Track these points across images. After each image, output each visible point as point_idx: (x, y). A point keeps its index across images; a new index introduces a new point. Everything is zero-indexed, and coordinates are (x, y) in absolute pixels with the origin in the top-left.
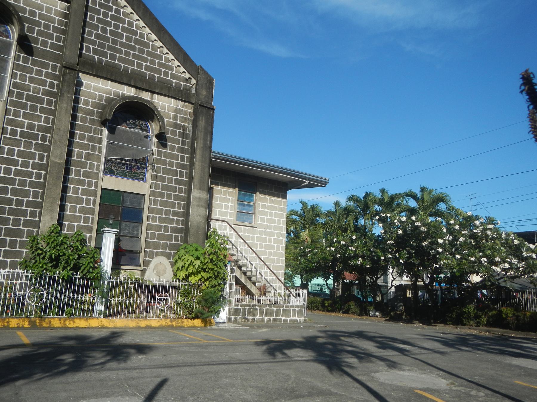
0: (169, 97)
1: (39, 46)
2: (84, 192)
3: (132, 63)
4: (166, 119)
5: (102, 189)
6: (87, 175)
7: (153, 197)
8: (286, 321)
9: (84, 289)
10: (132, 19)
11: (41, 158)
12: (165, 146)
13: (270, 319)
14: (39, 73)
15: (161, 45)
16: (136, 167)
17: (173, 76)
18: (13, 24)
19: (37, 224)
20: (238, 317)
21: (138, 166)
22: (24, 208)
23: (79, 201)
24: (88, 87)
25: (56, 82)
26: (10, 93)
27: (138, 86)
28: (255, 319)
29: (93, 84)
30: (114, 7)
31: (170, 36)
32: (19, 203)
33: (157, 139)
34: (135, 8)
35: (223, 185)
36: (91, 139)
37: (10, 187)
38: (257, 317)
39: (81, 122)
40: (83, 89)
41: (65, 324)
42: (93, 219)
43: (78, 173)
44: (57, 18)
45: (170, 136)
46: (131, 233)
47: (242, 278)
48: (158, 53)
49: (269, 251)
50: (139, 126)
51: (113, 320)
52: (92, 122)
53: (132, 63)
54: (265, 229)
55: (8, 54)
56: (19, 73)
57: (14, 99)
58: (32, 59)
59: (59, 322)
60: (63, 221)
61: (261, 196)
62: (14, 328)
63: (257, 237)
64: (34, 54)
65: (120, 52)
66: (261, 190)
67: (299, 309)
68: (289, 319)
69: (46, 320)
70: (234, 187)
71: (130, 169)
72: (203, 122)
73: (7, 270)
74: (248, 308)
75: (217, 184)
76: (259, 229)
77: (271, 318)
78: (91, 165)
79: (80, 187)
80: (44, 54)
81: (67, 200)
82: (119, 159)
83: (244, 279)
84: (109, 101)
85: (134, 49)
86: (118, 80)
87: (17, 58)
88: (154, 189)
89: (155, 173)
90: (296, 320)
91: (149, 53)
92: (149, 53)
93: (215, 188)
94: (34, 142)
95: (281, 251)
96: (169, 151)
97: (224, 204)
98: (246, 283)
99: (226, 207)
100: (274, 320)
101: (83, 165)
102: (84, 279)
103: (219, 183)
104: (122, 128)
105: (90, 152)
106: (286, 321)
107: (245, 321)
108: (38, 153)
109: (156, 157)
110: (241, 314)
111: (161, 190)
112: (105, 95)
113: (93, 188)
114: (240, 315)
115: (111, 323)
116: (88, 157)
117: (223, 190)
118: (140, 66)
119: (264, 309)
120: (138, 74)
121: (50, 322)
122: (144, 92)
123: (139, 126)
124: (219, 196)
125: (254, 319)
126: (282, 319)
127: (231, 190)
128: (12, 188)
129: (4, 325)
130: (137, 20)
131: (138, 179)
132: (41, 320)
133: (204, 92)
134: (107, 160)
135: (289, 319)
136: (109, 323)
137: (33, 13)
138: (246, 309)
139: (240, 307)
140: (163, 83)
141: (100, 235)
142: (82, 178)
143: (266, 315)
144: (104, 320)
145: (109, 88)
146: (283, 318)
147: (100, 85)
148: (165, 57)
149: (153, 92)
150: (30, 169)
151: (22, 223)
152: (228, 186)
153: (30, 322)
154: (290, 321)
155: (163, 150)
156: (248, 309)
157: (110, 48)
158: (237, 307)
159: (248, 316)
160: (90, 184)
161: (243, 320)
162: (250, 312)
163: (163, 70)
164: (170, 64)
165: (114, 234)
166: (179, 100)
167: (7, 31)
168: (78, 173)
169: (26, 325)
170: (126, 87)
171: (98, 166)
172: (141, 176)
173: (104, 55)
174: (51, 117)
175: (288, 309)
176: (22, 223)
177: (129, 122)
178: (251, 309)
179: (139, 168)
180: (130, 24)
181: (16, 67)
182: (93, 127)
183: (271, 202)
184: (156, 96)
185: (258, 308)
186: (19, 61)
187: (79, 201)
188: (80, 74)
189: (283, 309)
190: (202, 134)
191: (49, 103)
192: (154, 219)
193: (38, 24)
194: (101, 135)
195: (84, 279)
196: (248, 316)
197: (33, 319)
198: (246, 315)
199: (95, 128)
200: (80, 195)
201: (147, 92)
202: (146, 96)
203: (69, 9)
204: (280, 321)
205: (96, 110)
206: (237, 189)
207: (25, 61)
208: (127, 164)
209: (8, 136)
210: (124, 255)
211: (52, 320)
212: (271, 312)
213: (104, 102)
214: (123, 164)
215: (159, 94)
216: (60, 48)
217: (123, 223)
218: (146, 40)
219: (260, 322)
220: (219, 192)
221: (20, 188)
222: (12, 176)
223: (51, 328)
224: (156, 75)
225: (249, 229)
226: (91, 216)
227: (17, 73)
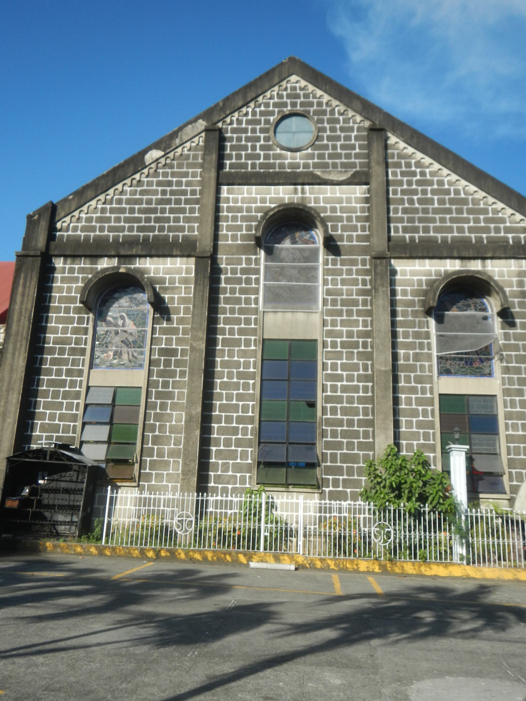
0: (506, 258)
1: (345, 243)
2: (419, 401)
3: (450, 230)
4: (507, 290)
5: (440, 395)
6: (418, 380)
7: (508, 396)
9: (437, 526)
10: (441, 176)
11: (365, 369)
12: (512, 325)
14: (349, 273)
15: (484, 194)
16: (479, 360)
17: (508, 230)
18: (316, 227)
19: (371, 447)
21: (480, 359)
22: (356, 428)
23: (415, 413)
24: (404, 273)
25: (368, 278)
26: (325, 301)
27: (463, 254)
29: (408, 269)
30: (418, 170)
31: (493, 180)
32: (350, 423)
33: (501, 318)
34: (443, 161)
36: (417, 335)
37: (339, 406)
39: (402, 317)
40: (398, 277)
41: (420, 571)
42: (434, 434)
43: (408, 380)
44: (358, 205)
45: (517, 309)
46: (485, 450)
50: (472, 306)
51: (480, 568)
52: (415, 314)
53: (450, 230)
55: (316, 260)
56: (330, 278)
57: (329, 307)
58: (341, 260)
59: (412, 567)
60: (399, 439)
62: (364, 572)
64: (342, 252)
65: (433, 220)
69: (398, 564)
71: (471, 364)
73: (349, 502)
78: (422, 367)
79: (414, 396)
80: (352, 250)
81: (400, 414)
82: (455, 354)
84: (431, 283)
85: (449, 211)
86: (437, 255)
87: (326, 263)
88: (507, 386)
89: (505, 364)
91: (470, 211)
92: (470, 211)
94: (356, 351)
96: (519, 331)
101: (412, 368)
102: (434, 513)
104: (452, 313)
105: (418, 351)
108: (361, 363)
109: (503, 342)
111: (519, 385)
112: (424, 278)
113: (428, 395)
115: (478, 573)
116: (417, 358)
118: (461, 230)
120: (460, 241)
121: (403, 567)
122: (472, 261)
123: (472, 306)
128: (341, 408)
129: (353, 568)
130: (448, 175)
131: (483, 375)
132: (392, 564)
134: (440, 358)
136: (476, 572)
137: (333, 210)
140: (495, 242)
141: (446, 454)
142: (413, 384)
144: (467, 567)
145: (427, 268)
147: (417, 268)
148: (492, 209)
149: (484, 258)
150: (355, 383)
151: (356, 446)
153: (381, 566)
155: (511, 331)
157: (421, 220)
160: (423, 391)
163: (492, 226)
164: (500, 215)
165: (464, 453)
166: (522, 258)
167: (312, 237)
168: (408, 380)
169: (377, 569)
170: (448, 261)
171: (431, 366)
172: (487, 371)
173: (416, 230)
174: (369, 319)
176: (356, 446)
177: (460, 304)
179: (482, 361)
180: (441, 183)
181: (327, 272)
182: (417, 320)
184: (489, 262)
186: (327, 265)
187: (415, 413)
188: (393, 261)
191: (365, 303)
192: (515, 427)
193: (340, 219)
194: (428, 328)
195: (434, 513)
197: (383, 563)
199: (419, 321)
200: (414, 406)
201: (476, 261)
202: (475, 266)
203: (369, 191)
205: (416, 299)
207: (334, 263)
208: (466, 358)
209: (329, 349)
210: (481, 479)
211: (405, 565)
213: (424, 287)
214: (461, 359)
215: (492, 258)
216: (367, 238)
217: (473, 436)
221: (348, 405)
222: (339, 394)
223: (404, 575)
224: (484, 236)
226: (431, 431)
227: (327, 279)
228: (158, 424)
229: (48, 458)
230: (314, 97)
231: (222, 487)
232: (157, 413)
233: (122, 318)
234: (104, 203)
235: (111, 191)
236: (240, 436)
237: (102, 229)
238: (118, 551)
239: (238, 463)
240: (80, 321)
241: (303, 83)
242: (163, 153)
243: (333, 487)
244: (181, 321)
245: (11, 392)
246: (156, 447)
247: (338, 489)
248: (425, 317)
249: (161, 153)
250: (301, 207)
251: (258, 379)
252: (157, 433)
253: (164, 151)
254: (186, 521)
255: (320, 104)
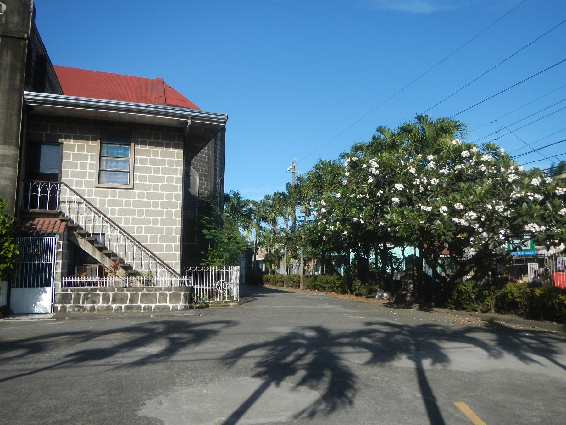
13: (121, 307)
20: (68, 306)
28: (96, 307)
35: (76, 138)
38: (98, 305)
47: (95, 255)
49: (153, 219)
54: (146, 190)
61: (139, 147)
63: (133, 201)
66: (139, 140)
67: (173, 293)
68: (153, 306)
70: (94, 139)
72: (9, 56)
74: (84, 293)
75: (68, 138)
76: (137, 191)
77: (123, 306)
83: (99, 256)
90: (168, 308)
93: (65, 143)
95: (174, 217)
97: (79, 162)
98: (103, 261)
99: (83, 166)
100: (128, 308)
103: (71, 135)
106: (147, 309)
107: (79, 310)
110: (72, 301)
114: (70, 303)
117: (78, 145)
119: (111, 294)
124: (72, 153)
125: (94, 307)
126: (141, 307)
127: (90, 143)
133: (16, 19)
135: (153, 306)
138: (80, 295)
139: (71, 293)
143: (114, 301)
146: (143, 305)
152: (87, 139)
154: (154, 309)
156: (84, 295)
158: (66, 293)
159: (83, 303)
161: (76, 309)
162: (86, 298)
175: (152, 292)
178: (88, 294)
183: (156, 154)
185: (101, 293)
189: (142, 292)
190: (7, 72)
196: (83, 303)
198: (81, 303)
204: (137, 309)
206: (98, 142)
212: (123, 297)
219: (104, 310)
220: (72, 148)
225: (120, 191)
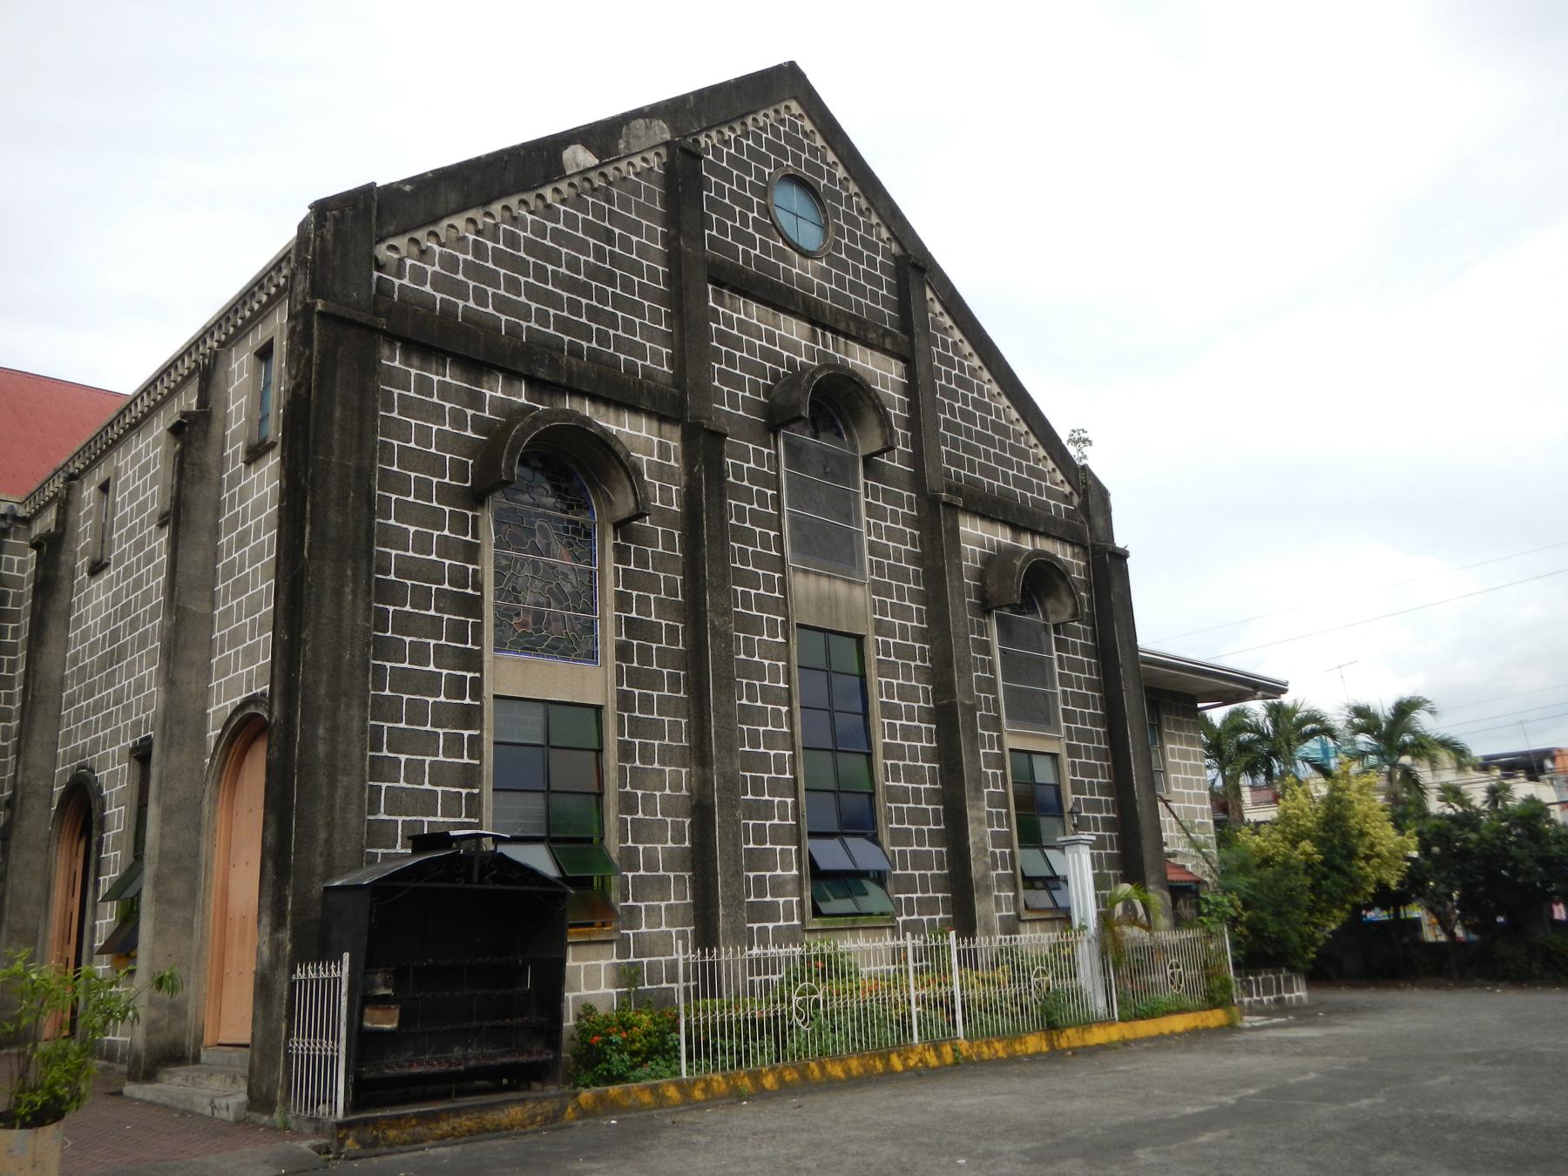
8: (1290, 999)
48: (1023, 446)
94: (913, 664)
112: (978, 549)
129: (1022, 1051)
143: (1266, 993)
169: (1045, 1049)
180: (981, 392)
213: (979, 566)
218: (1004, 422)
228: (640, 793)
229: (475, 880)
230: (824, 160)
231: (758, 928)
232: (637, 768)
233: (545, 535)
234: (478, 233)
235: (496, 208)
236: (776, 821)
237: (481, 298)
238: (715, 1084)
239: (778, 876)
240: (460, 523)
241: (808, 126)
242: (597, 161)
243: (908, 915)
244: (661, 561)
245: (344, 700)
246: (641, 847)
247: (913, 918)
248: (984, 618)
249: (592, 160)
250: (857, 380)
251: (796, 704)
252: (640, 815)
253: (600, 159)
254: (810, 999)
255: (832, 177)
